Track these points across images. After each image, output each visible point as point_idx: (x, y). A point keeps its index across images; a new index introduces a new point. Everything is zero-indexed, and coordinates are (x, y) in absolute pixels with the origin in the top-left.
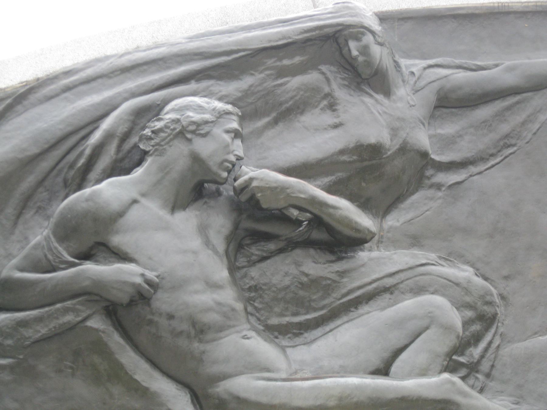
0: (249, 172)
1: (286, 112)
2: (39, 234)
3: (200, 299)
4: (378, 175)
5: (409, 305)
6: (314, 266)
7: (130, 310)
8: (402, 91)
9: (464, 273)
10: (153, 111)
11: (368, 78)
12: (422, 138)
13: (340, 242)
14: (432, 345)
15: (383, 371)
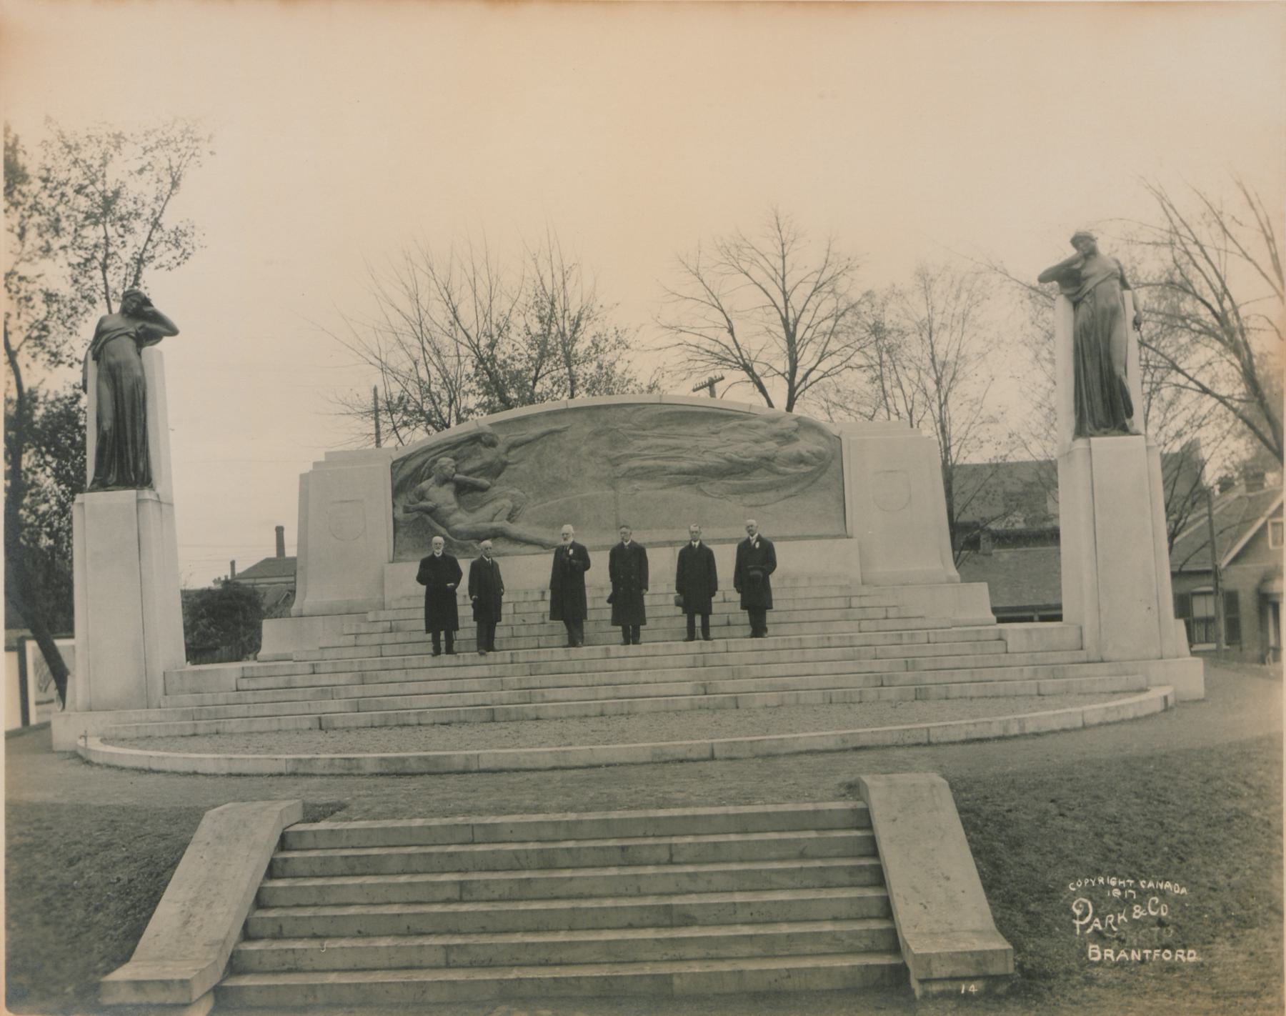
0: (458, 476)
1: (469, 457)
2: (411, 496)
3: (447, 508)
4: (494, 470)
5: (498, 504)
6: (479, 495)
7: (431, 511)
8: (499, 446)
9: (516, 491)
10: (435, 461)
11: (492, 444)
12: (504, 458)
13: (483, 489)
14: (505, 512)
15: (492, 521)
